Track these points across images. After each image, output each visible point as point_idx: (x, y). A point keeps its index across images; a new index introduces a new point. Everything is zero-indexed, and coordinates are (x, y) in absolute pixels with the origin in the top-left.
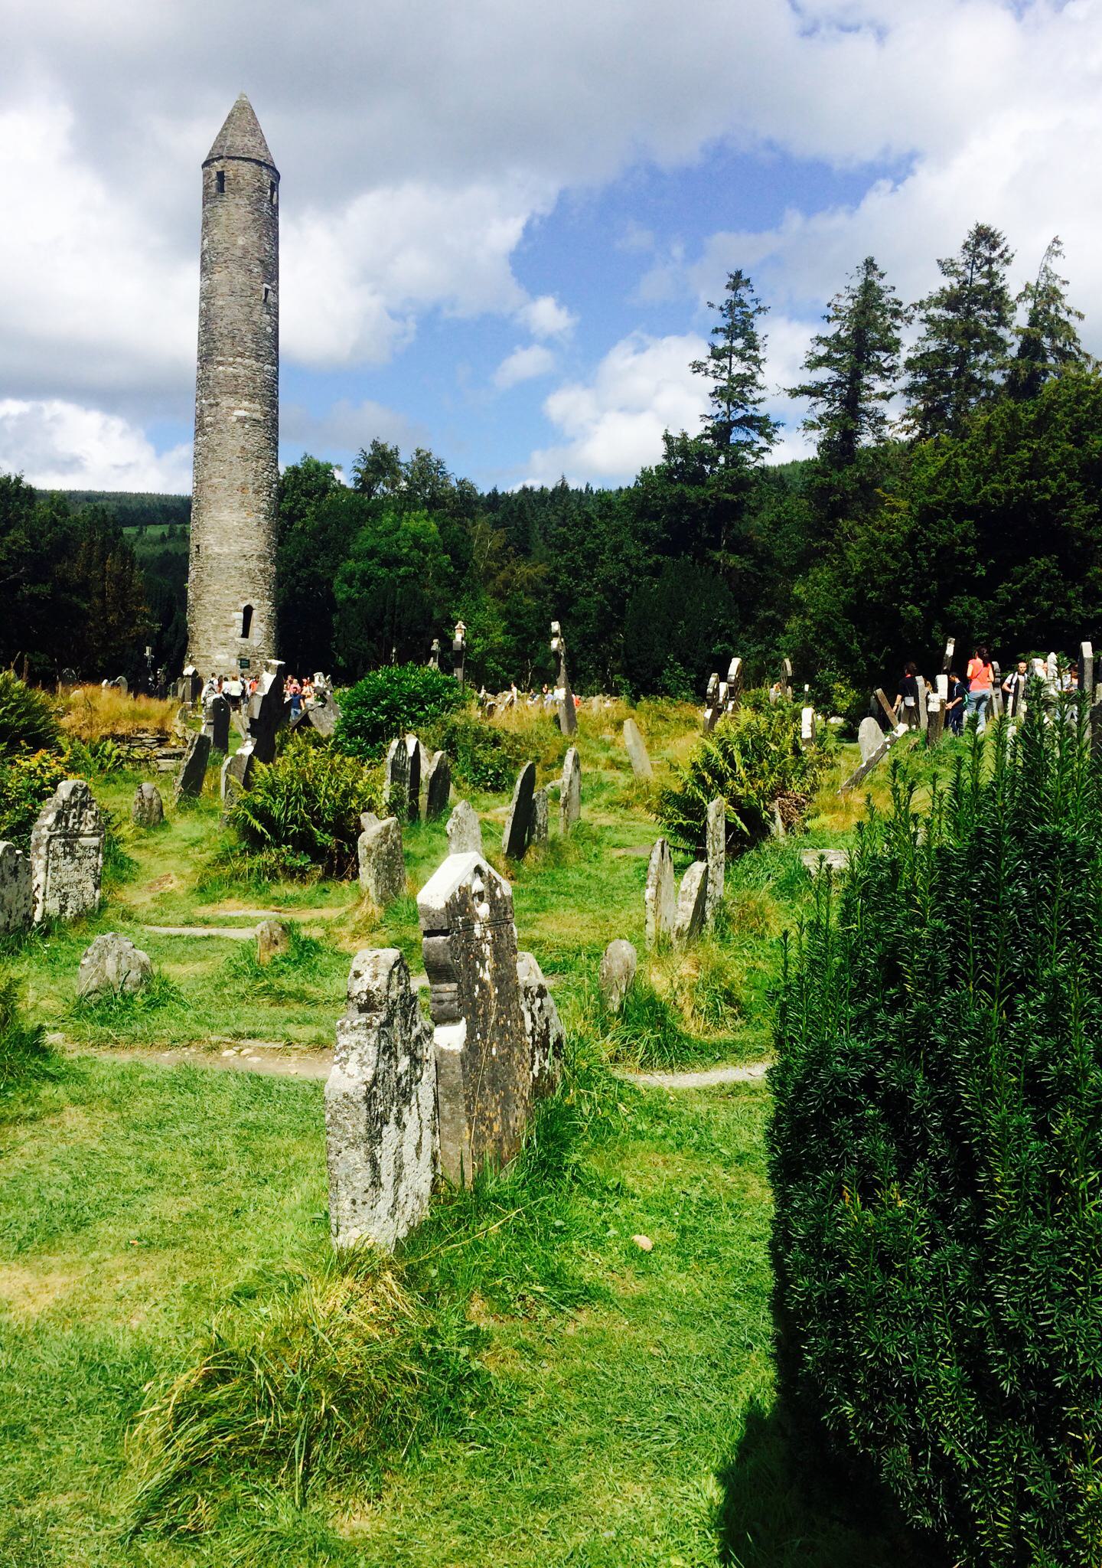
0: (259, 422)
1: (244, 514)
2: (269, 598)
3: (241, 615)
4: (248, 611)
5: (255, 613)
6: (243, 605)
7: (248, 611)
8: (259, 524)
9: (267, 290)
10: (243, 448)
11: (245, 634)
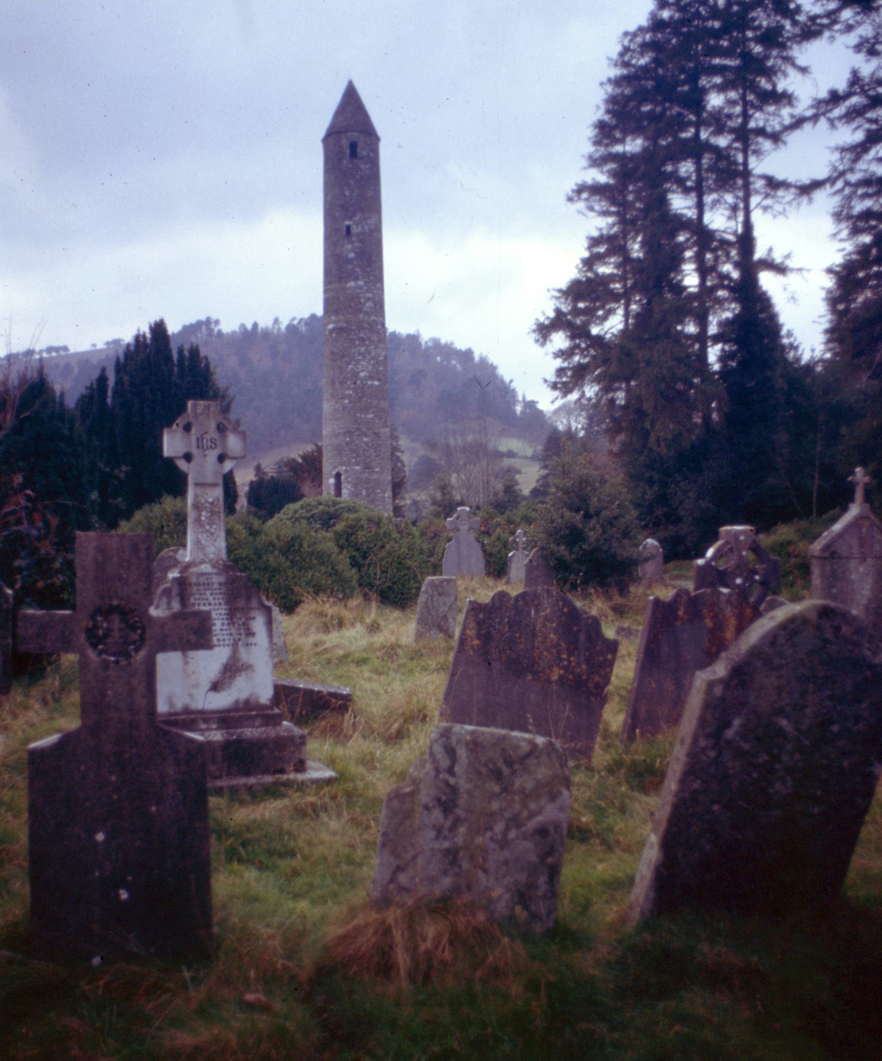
0: (342, 329)
1: (333, 403)
2: (357, 464)
3: (332, 481)
4: (338, 476)
5: (343, 478)
6: (334, 473)
7: (338, 476)
8: (344, 408)
9: (348, 228)
10: (332, 353)
11: (338, 492)
